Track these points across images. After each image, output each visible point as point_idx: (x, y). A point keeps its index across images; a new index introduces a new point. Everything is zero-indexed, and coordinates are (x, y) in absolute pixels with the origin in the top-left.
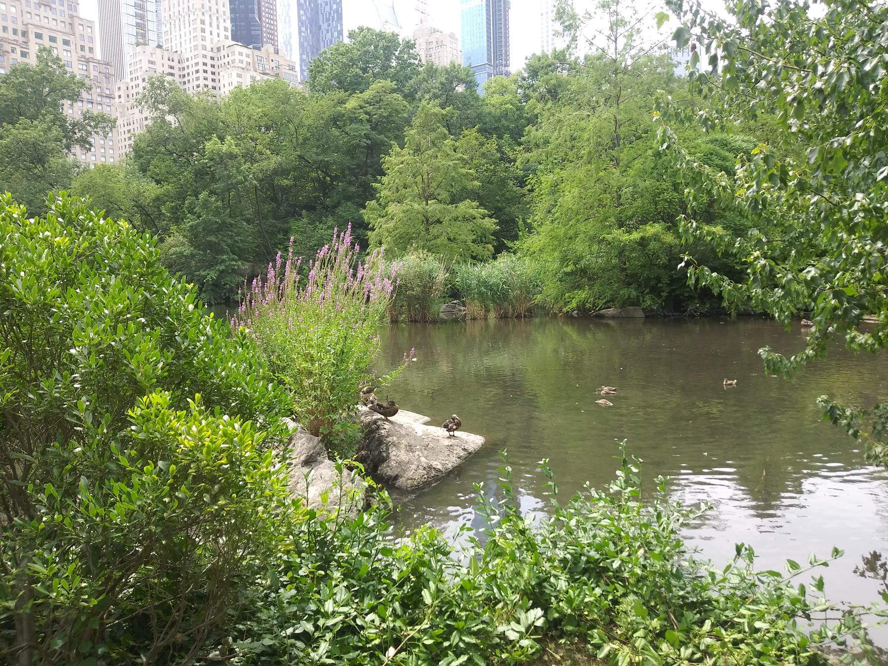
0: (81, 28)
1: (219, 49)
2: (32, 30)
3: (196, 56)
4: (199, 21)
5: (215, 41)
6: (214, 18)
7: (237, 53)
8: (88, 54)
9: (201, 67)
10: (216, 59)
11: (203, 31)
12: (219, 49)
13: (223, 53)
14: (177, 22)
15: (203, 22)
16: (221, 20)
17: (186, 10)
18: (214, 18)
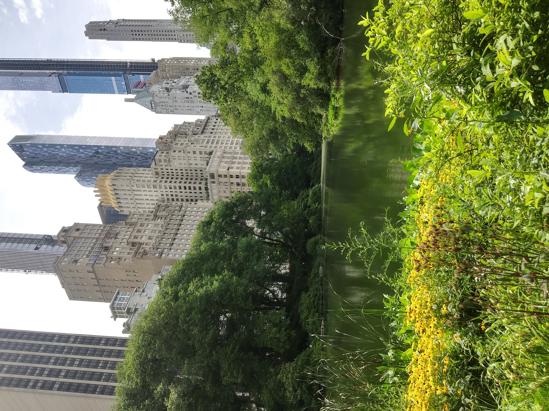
0: (133, 219)
1: (157, 173)
2: (132, 240)
3: (160, 187)
4: (138, 183)
5: (152, 176)
6: (137, 175)
7: (160, 158)
8: (152, 217)
9: (168, 184)
10: (163, 176)
11: (144, 181)
12: (157, 173)
13: (159, 170)
14: (138, 202)
15: (138, 181)
16: (138, 172)
17: (130, 193)
18: (137, 175)
